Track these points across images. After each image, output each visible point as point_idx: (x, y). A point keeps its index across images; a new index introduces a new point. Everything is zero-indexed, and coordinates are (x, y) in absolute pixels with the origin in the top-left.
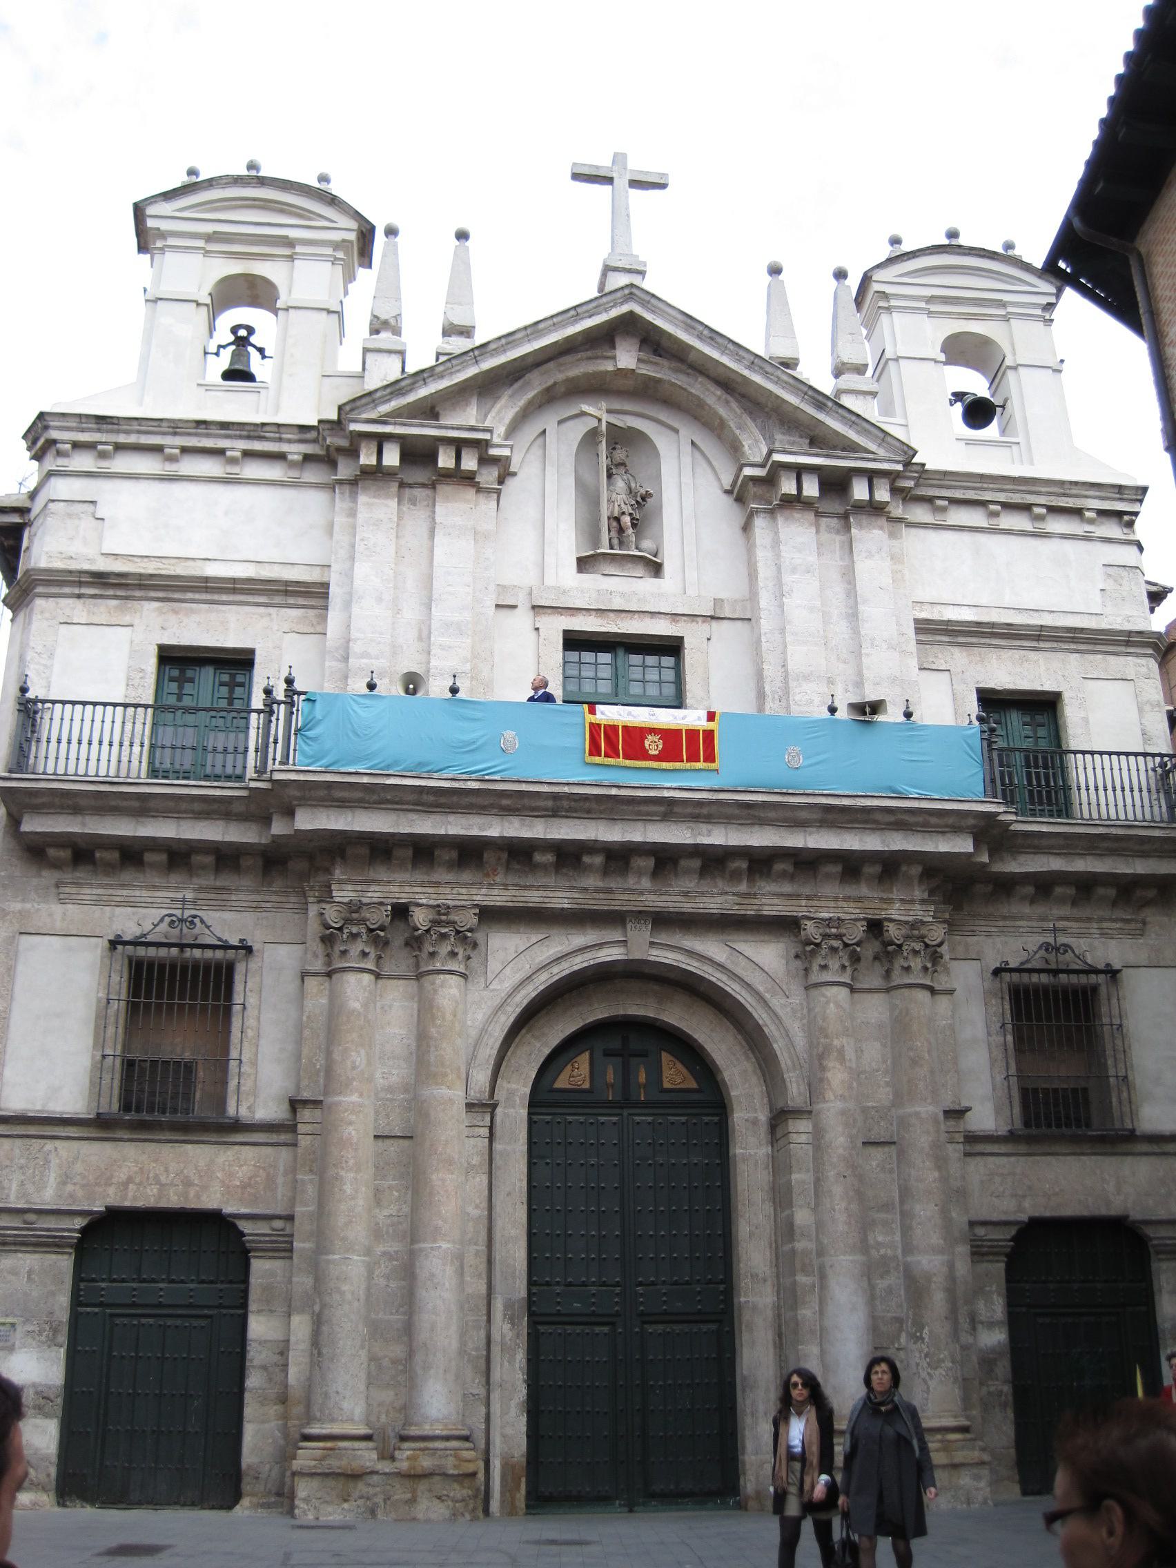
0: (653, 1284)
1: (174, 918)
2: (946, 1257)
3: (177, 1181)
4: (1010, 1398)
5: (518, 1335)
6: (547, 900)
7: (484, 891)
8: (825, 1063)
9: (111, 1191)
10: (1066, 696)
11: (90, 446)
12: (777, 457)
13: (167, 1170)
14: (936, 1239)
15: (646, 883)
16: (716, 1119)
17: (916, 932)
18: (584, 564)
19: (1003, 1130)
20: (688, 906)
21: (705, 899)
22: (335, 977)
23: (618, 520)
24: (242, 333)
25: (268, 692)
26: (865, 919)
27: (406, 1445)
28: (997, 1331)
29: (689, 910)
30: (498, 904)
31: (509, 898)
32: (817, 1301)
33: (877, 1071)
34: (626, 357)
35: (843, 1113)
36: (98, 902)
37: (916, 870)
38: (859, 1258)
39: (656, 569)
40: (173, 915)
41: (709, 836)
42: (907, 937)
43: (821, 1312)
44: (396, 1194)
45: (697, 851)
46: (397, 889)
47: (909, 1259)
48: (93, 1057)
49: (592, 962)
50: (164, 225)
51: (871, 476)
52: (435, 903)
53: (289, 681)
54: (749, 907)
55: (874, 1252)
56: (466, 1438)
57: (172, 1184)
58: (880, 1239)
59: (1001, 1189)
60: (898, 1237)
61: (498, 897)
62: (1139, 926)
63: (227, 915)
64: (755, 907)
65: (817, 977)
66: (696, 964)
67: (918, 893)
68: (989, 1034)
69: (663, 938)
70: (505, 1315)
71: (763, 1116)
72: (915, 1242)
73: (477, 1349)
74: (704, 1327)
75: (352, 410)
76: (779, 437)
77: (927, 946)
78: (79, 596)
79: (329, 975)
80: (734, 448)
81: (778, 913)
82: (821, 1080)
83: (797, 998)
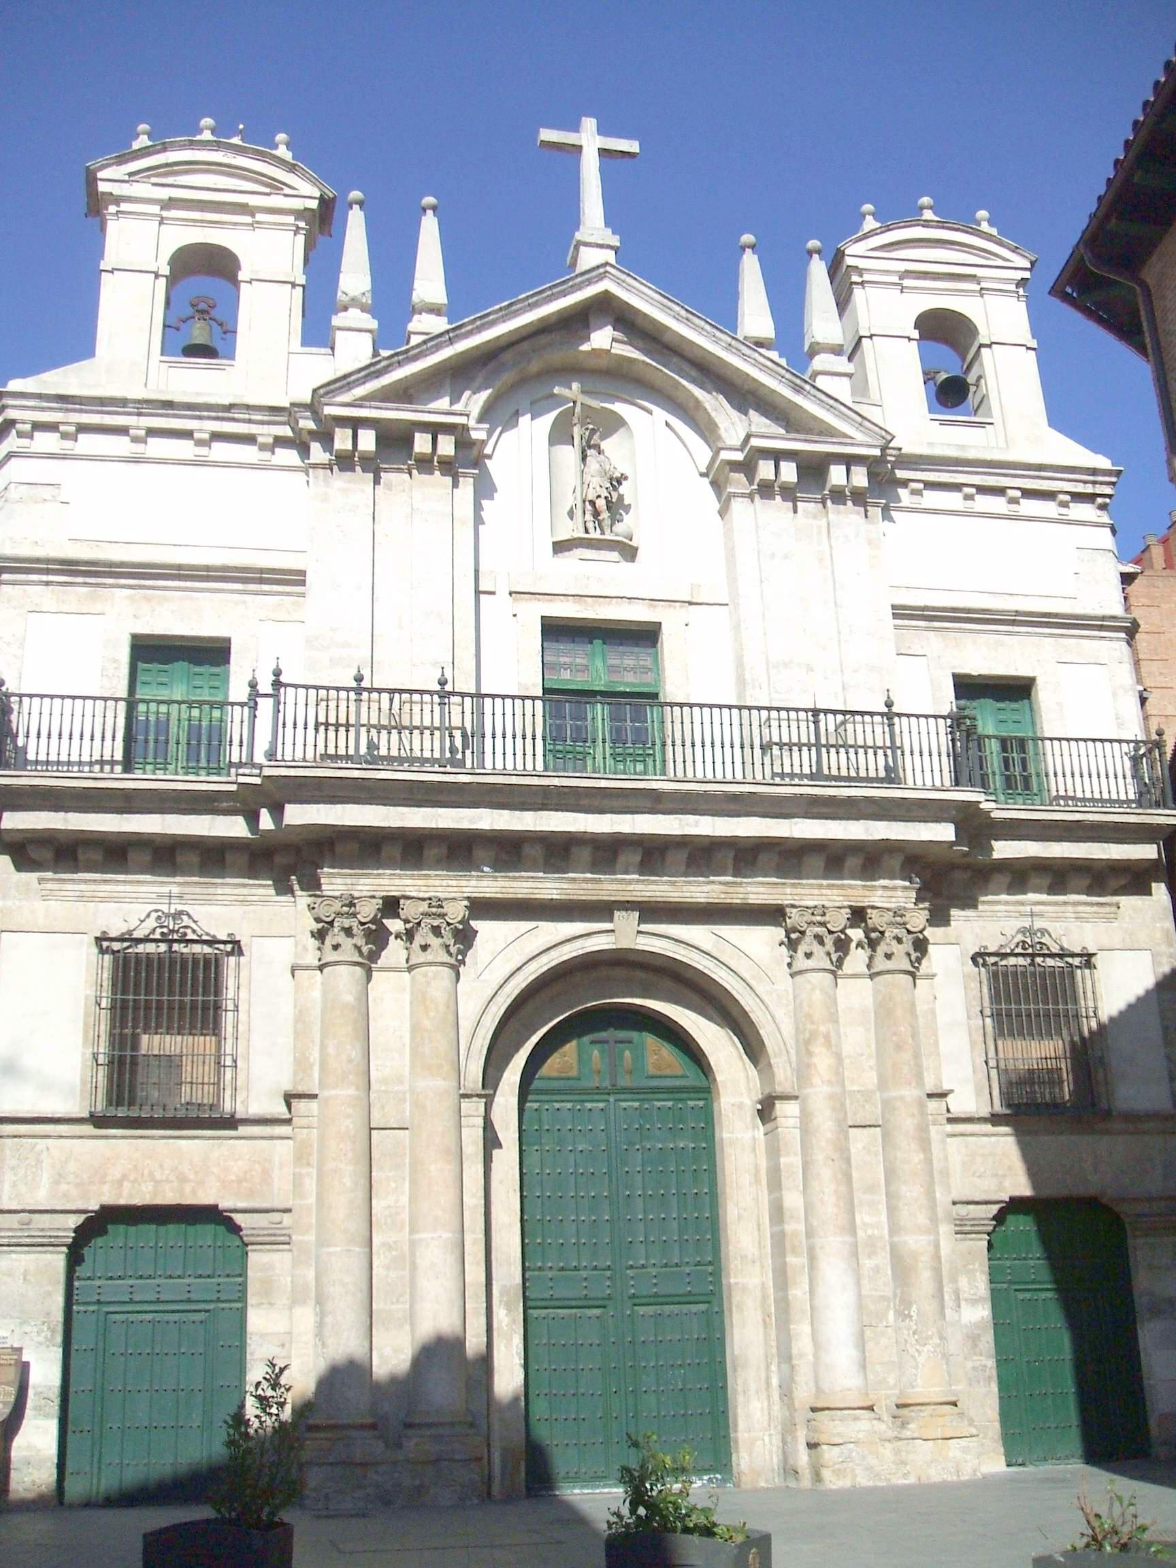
0: (643, 1266)
1: (160, 914)
2: (932, 1237)
3: (172, 1178)
4: (994, 1373)
5: (514, 1321)
6: (536, 891)
7: (473, 883)
8: (811, 1048)
9: (106, 1188)
10: (1039, 682)
11: (52, 427)
12: (755, 442)
13: (161, 1166)
16: (701, 1103)
17: (898, 919)
19: (985, 1111)
21: (693, 888)
22: (326, 970)
23: (592, 503)
24: (203, 306)
25: (253, 685)
26: (850, 907)
27: (410, 1432)
28: (980, 1307)
29: (677, 900)
30: (488, 895)
31: (498, 890)
32: (807, 1281)
33: (862, 1055)
35: (831, 1097)
36: (81, 898)
38: (848, 1239)
39: (629, 552)
40: (157, 911)
41: (696, 826)
42: (890, 924)
43: (812, 1292)
44: (393, 1185)
45: (683, 842)
46: (386, 882)
47: (896, 1239)
48: (83, 1054)
49: (581, 952)
50: (116, 189)
51: (849, 461)
52: (427, 895)
53: (277, 673)
54: (735, 895)
55: (860, 1233)
56: (472, 1425)
57: (168, 1181)
58: (867, 1219)
59: (982, 1169)
60: (884, 1218)
62: (1114, 909)
64: (741, 896)
65: (801, 963)
66: (682, 952)
68: (969, 1018)
70: (500, 1301)
72: (902, 1223)
73: (477, 1336)
74: (694, 1308)
75: (327, 393)
77: (909, 932)
78: (47, 583)
79: (321, 968)
80: (706, 429)
81: (764, 902)
82: (808, 1066)
83: (784, 982)
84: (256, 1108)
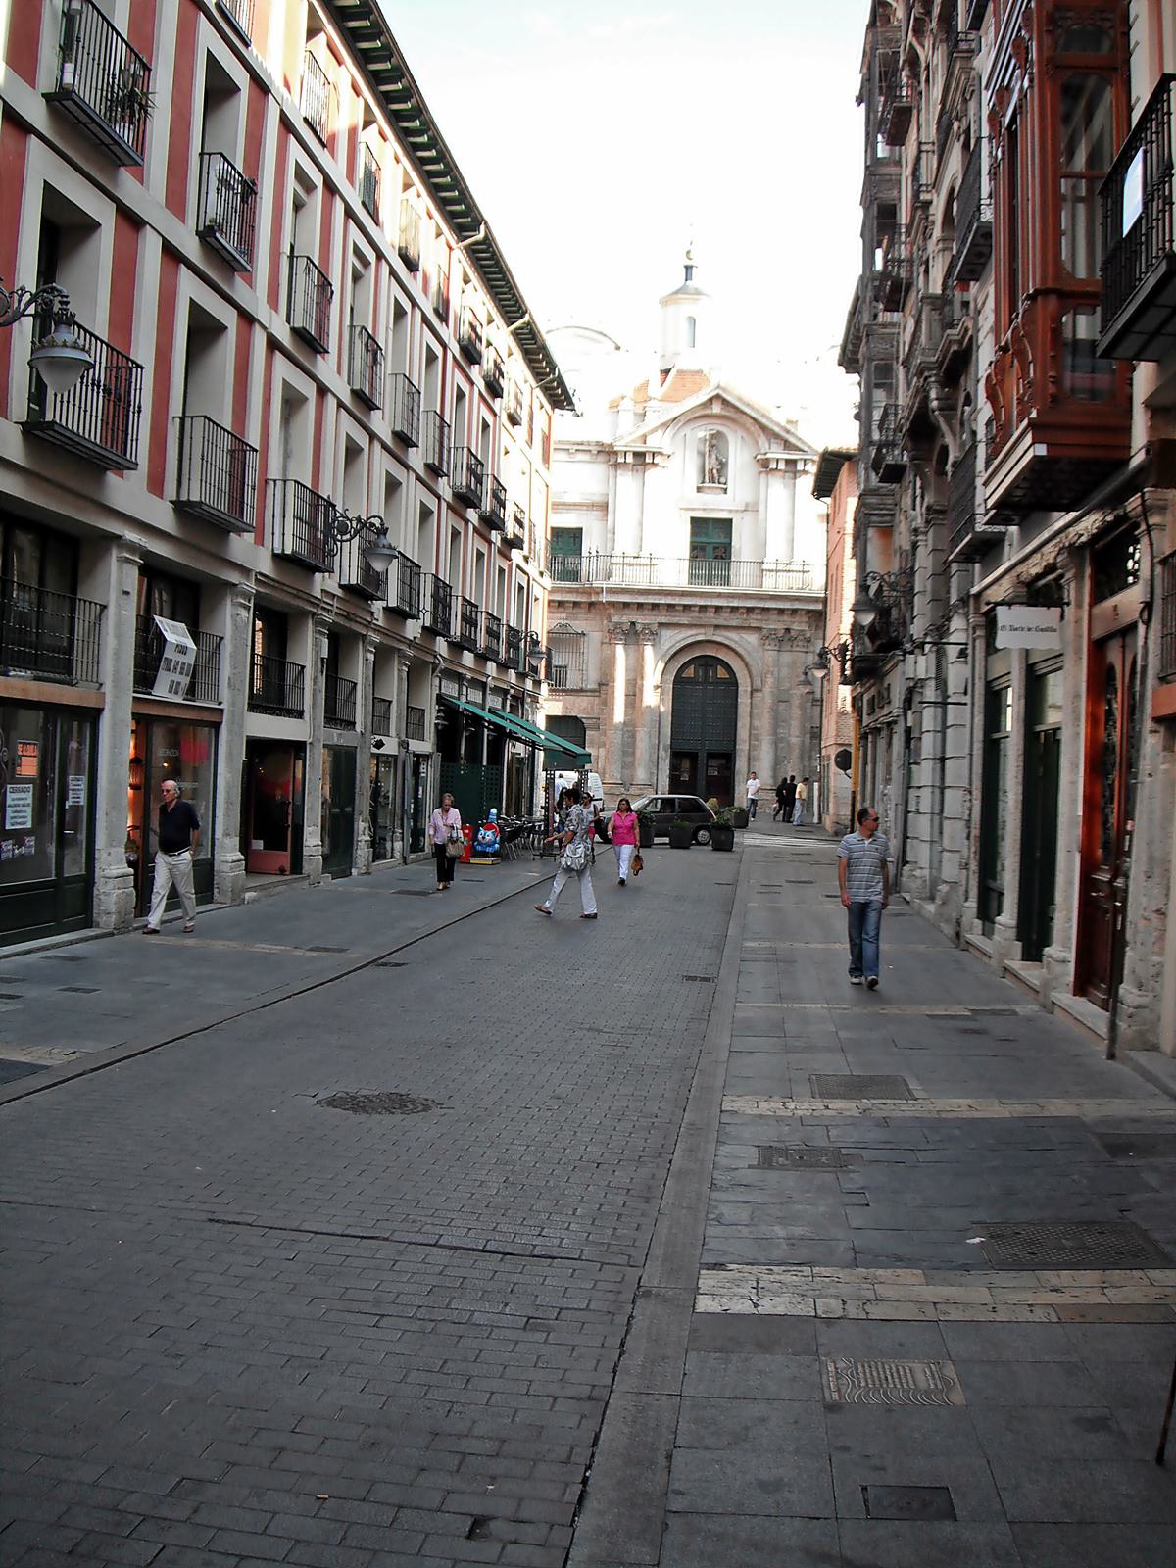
14: (797, 733)
15: (712, 615)
18: (699, 490)
20: (726, 623)
34: (717, 409)
35: (772, 692)
37: (803, 612)
61: (664, 620)
63: (577, 622)
67: (805, 619)
69: (718, 632)
71: (749, 689)
76: (773, 440)
84: (589, 687)
